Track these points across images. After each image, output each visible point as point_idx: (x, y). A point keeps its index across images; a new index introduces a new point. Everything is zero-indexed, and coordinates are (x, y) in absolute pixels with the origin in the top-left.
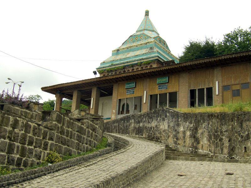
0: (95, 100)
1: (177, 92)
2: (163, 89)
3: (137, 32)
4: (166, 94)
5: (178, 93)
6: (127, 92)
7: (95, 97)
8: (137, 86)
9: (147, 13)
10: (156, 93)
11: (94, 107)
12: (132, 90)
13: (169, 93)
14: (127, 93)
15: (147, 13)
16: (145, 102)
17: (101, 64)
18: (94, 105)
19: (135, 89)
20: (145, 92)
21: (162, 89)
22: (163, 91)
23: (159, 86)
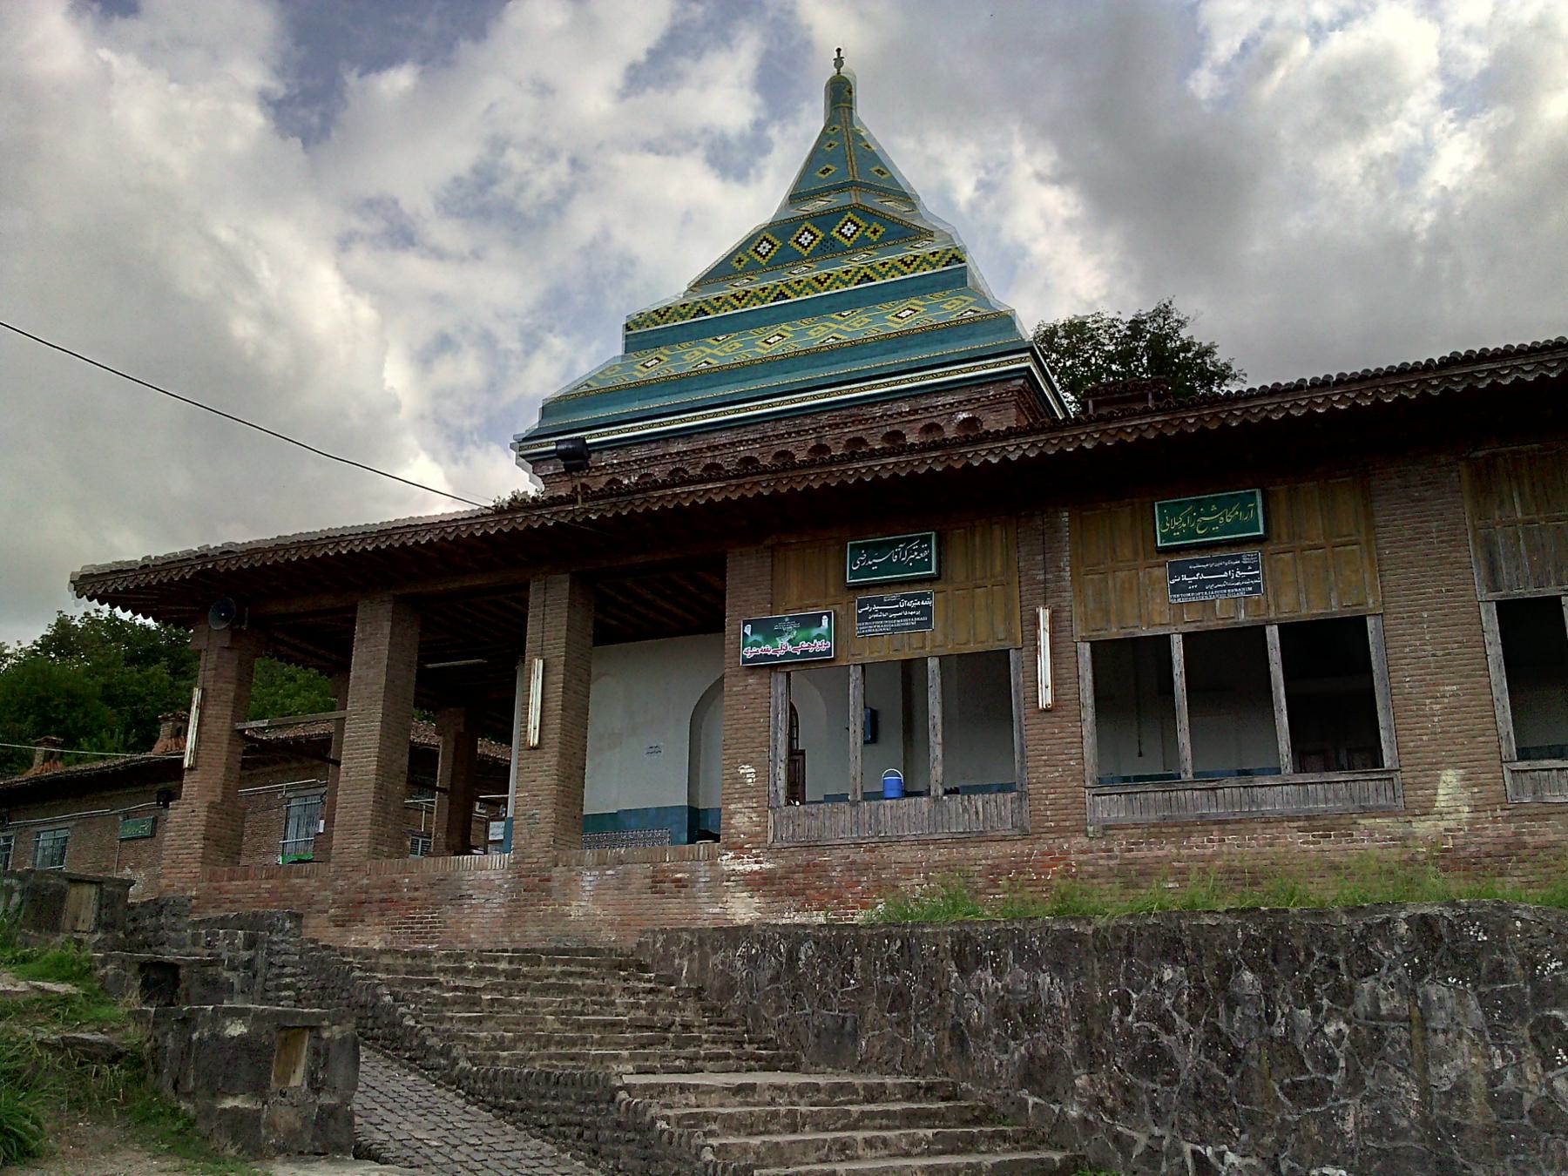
0: (557, 678)
1: (1361, 621)
2: (1220, 599)
3: (795, 197)
4: (1258, 632)
5: (1370, 622)
6: (863, 618)
7: (558, 652)
8: (958, 568)
10: (1145, 632)
11: (554, 737)
12: (909, 598)
13: (1281, 626)
14: (869, 628)
16: (1045, 698)
17: (546, 411)
18: (555, 723)
19: (937, 587)
20: (1044, 615)
22: (1228, 607)
23: (1176, 570)
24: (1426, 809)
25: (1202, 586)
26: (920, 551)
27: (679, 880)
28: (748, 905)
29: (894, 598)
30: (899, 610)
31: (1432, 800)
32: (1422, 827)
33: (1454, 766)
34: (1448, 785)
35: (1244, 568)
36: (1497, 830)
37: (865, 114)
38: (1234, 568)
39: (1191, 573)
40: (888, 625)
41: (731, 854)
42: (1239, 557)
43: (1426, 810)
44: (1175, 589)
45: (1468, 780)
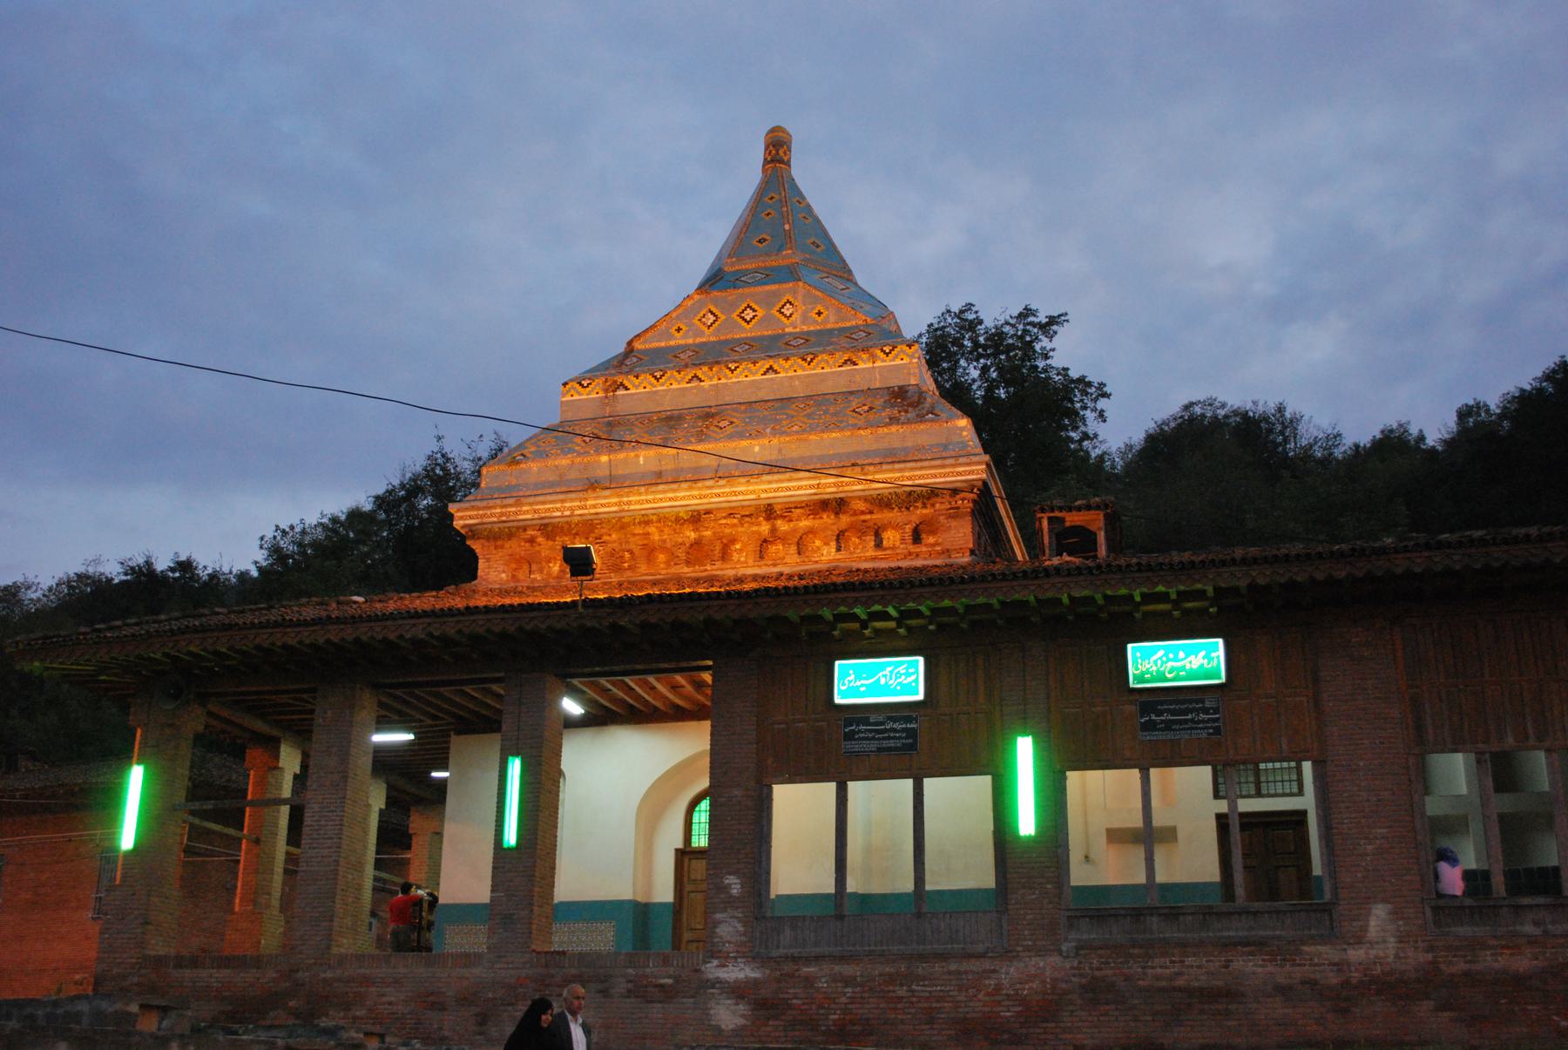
6: (850, 737)
9: (777, 148)
14: (856, 746)
15: (777, 148)
21: (1169, 736)
24: (1359, 940)
25: (1168, 726)
26: (908, 675)
27: (662, 986)
28: (734, 1012)
29: (881, 719)
30: (886, 731)
31: (1364, 929)
32: (1356, 954)
33: (1385, 901)
34: (1378, 918)
35: (1206, 711)
36: (1417, 957)
37: (803, 171)
38: (1198, 711)
39: (1160, 714)
40: (873, 746)
41: (715, 962)
42: (1202, 701)
43: (1359, 940)
44: (1149, 727)
45: (1396, 914)
